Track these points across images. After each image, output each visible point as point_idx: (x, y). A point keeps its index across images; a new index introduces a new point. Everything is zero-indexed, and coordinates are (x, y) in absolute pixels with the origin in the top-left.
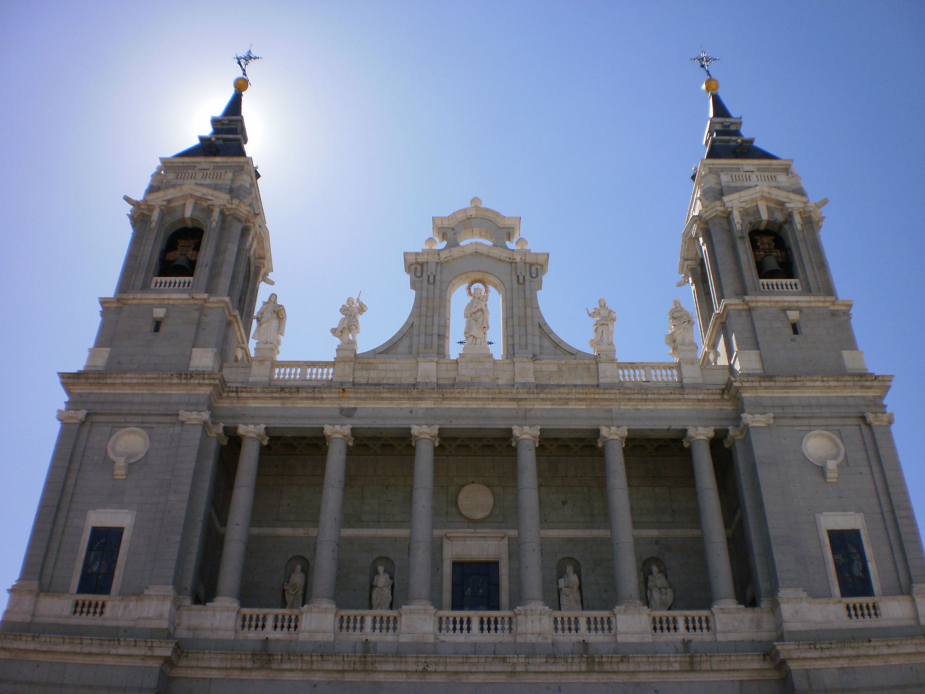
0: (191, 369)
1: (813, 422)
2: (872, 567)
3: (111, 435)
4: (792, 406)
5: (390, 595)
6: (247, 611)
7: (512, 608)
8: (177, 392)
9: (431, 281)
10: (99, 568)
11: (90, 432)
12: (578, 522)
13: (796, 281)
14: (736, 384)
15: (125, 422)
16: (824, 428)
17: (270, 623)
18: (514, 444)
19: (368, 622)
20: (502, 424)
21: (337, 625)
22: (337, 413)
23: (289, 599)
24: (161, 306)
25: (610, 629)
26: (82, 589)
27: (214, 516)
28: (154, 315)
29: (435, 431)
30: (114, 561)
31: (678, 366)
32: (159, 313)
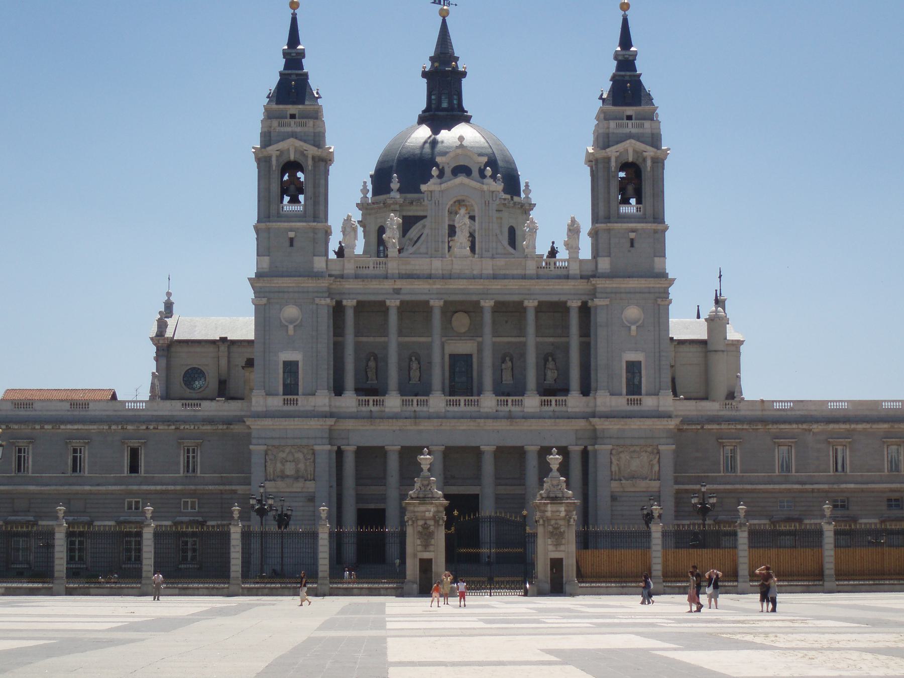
0: (315, 270)
2: (644, 380)
3: (281, 310)
4: (621, 293)
7: (479, 395)
8: (310, 284)
9: (437, 204)
10: (291, 381)
13: (641, 205)
17: (371, 403)
20: (474, 298)
21: (401, 403)
22: (391, 291)
23: (370, 374)
24: (291, 231)
25: (522, 404)
26: (284, 394)
28: (290, 236)
29: (442, 303)
31: (568, 261)
32: (292, 234)
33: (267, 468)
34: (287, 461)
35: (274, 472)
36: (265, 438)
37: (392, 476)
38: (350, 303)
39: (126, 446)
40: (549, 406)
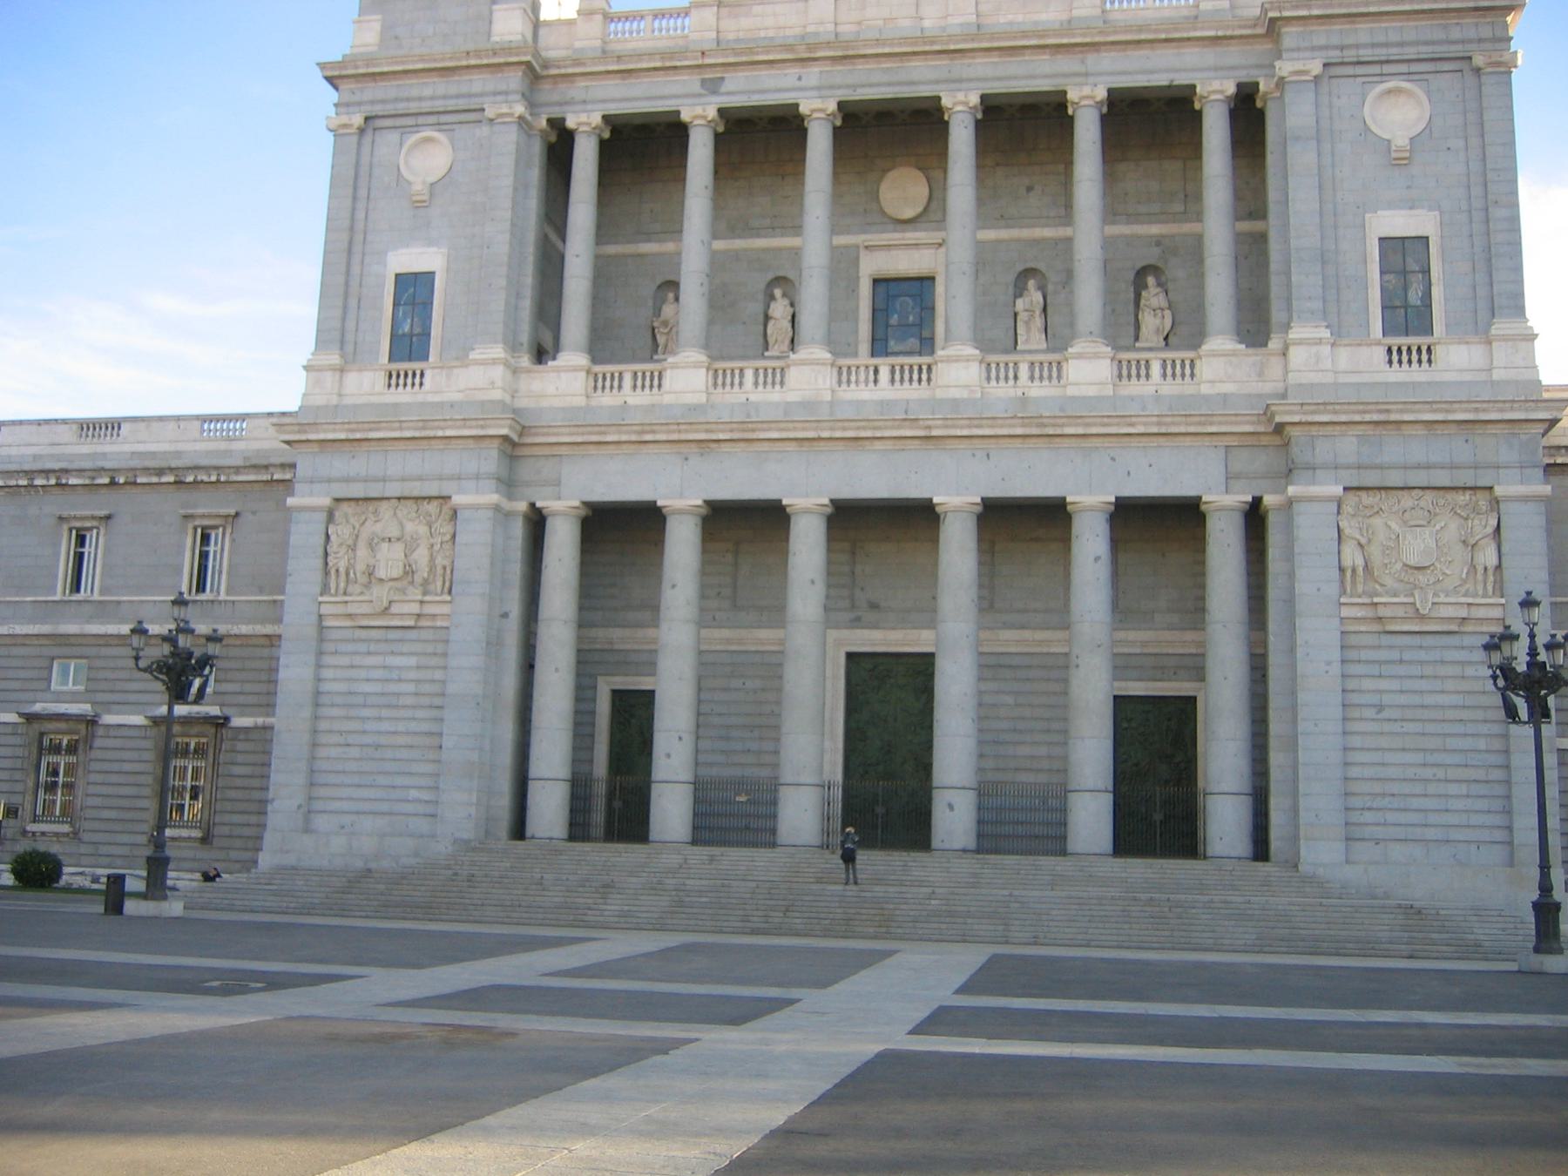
0: (495, 38)
1: (1387, 69)
2: (1437, 292)
3: (401, 144)
4: (1357, 46)
5: (790, 329)
6: (598, 369)
11: (373, 142)
12: (1048, 217)
14: (1271, 14)
15: (417, 126)
16: (1405, 77)
18: (946, 118)
19: (749, 374)
20: (925, 91)
22: (696, 87)
26: (392, 358)
27: (553, 237)
29: (832, 106)
30: (430, 317)
33: (329, 558)
34: (383, 540)
35: (347, 574)
36: (329, 481)
37: (674, 586)
38: (585, 121)
39: (65, 527)
40: (1143, 379)
